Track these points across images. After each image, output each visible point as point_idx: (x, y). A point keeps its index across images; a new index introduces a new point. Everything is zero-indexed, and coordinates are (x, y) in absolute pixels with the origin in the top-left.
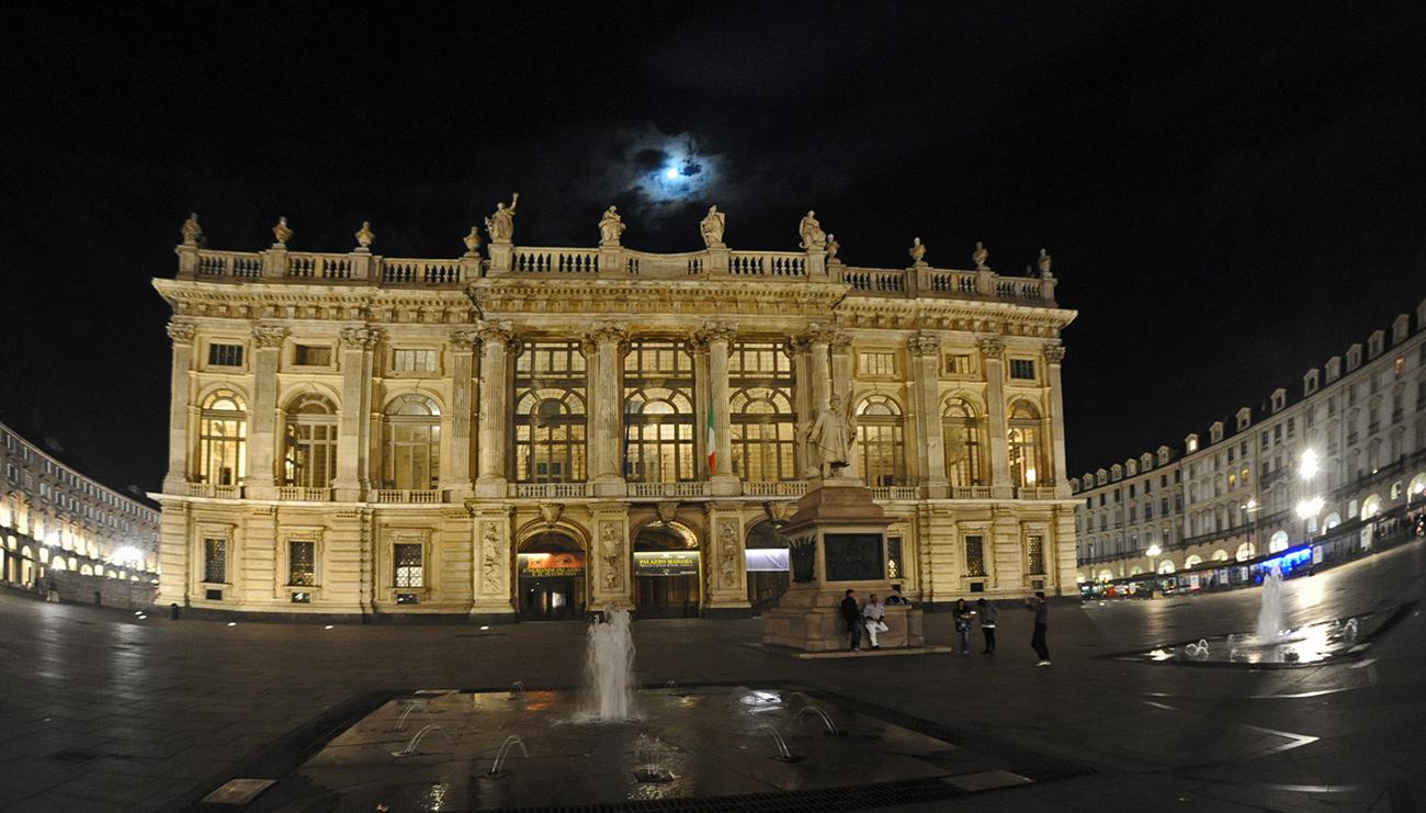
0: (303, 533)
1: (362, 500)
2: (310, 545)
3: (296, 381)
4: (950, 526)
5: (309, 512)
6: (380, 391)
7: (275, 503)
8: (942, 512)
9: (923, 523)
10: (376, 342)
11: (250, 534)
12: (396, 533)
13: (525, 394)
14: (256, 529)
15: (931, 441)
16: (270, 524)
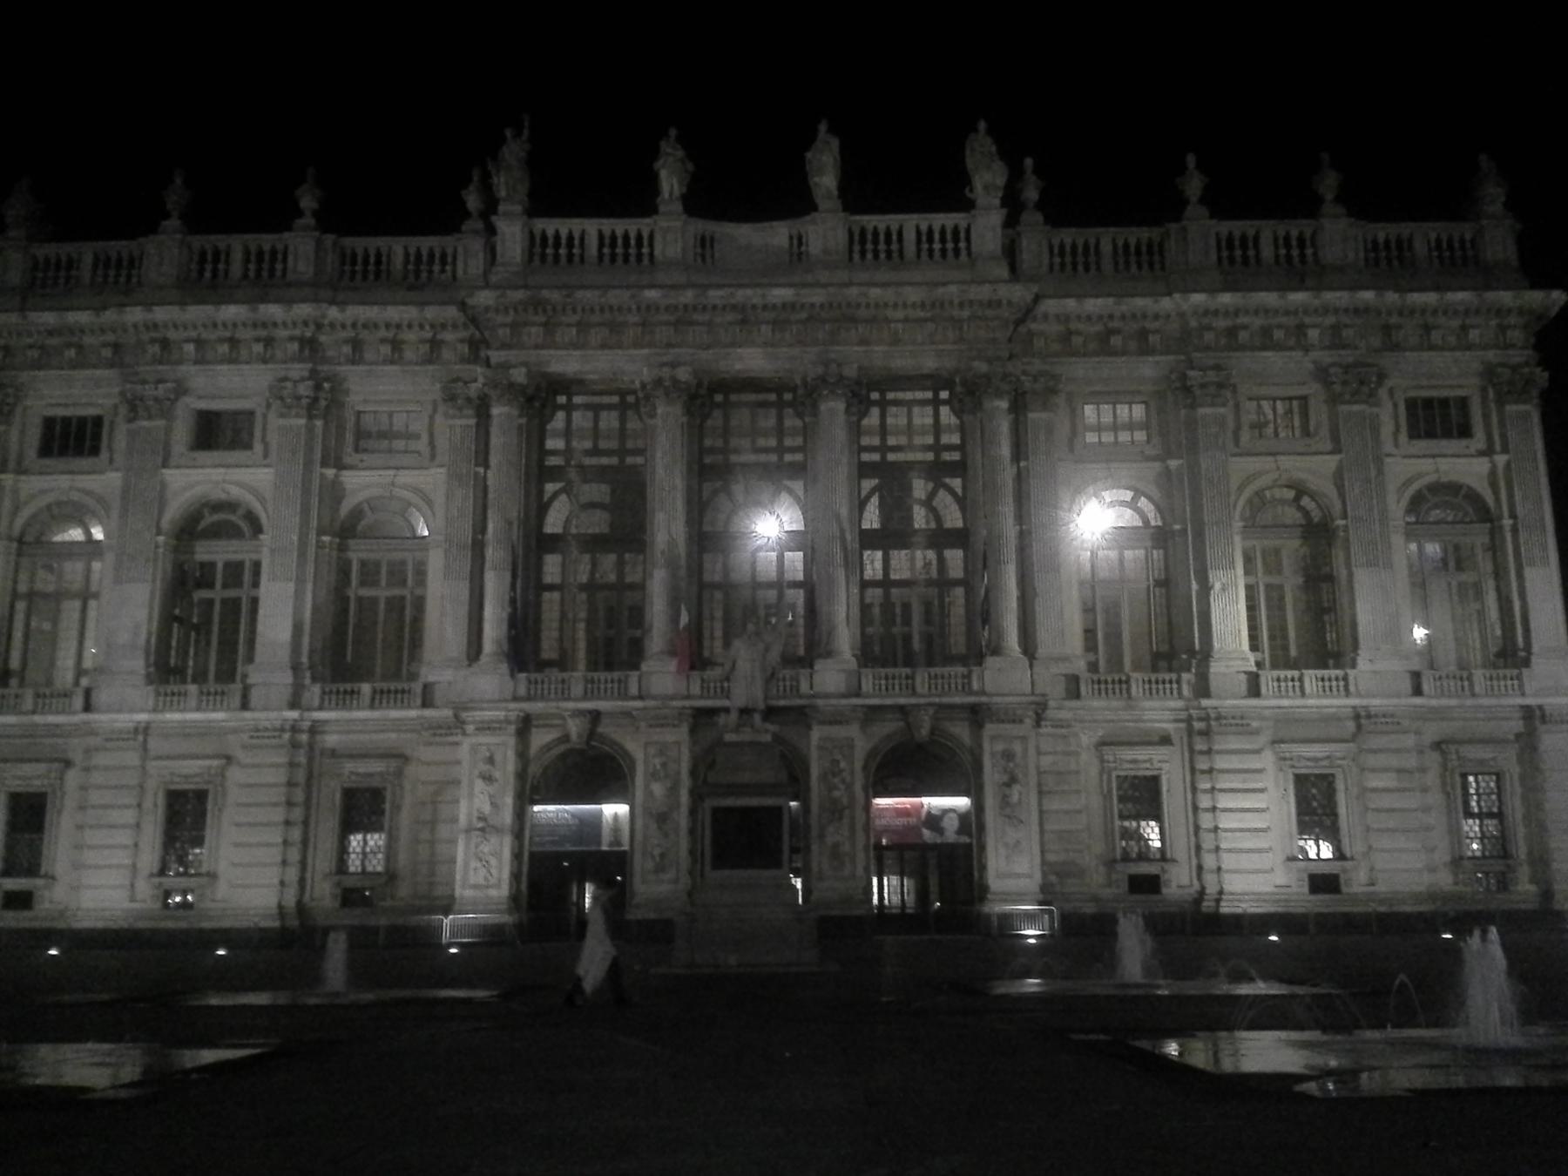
0: (190, 771)
1: (294, 704)
2: (201, 796)
3: (195, 480)
4: (1258, 752)
5: (205, 731)
6: (334, 493)
7: (143, 717)
8: (1241, 725)
9: (1200, 745)
10: (324, 401)
11: (97, 778)
12: (349, 766)
13: (555, 495)
14: (106, 768)
15: (1217, 580)
16: (132, 758)
